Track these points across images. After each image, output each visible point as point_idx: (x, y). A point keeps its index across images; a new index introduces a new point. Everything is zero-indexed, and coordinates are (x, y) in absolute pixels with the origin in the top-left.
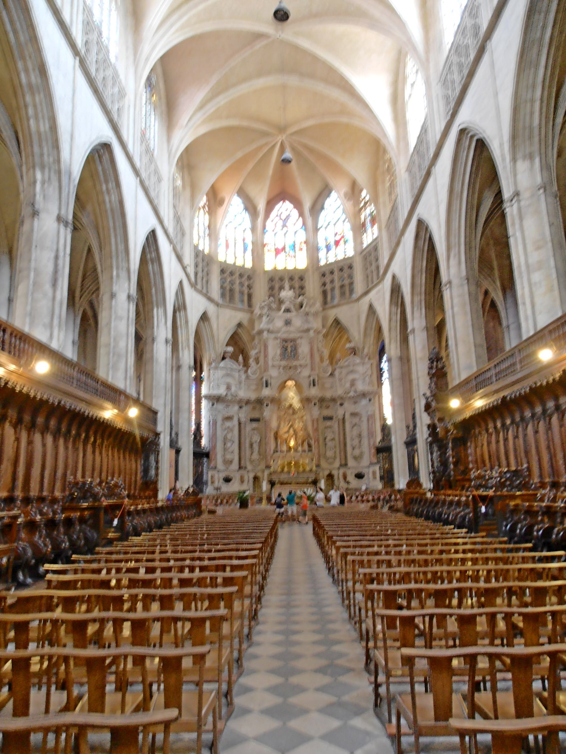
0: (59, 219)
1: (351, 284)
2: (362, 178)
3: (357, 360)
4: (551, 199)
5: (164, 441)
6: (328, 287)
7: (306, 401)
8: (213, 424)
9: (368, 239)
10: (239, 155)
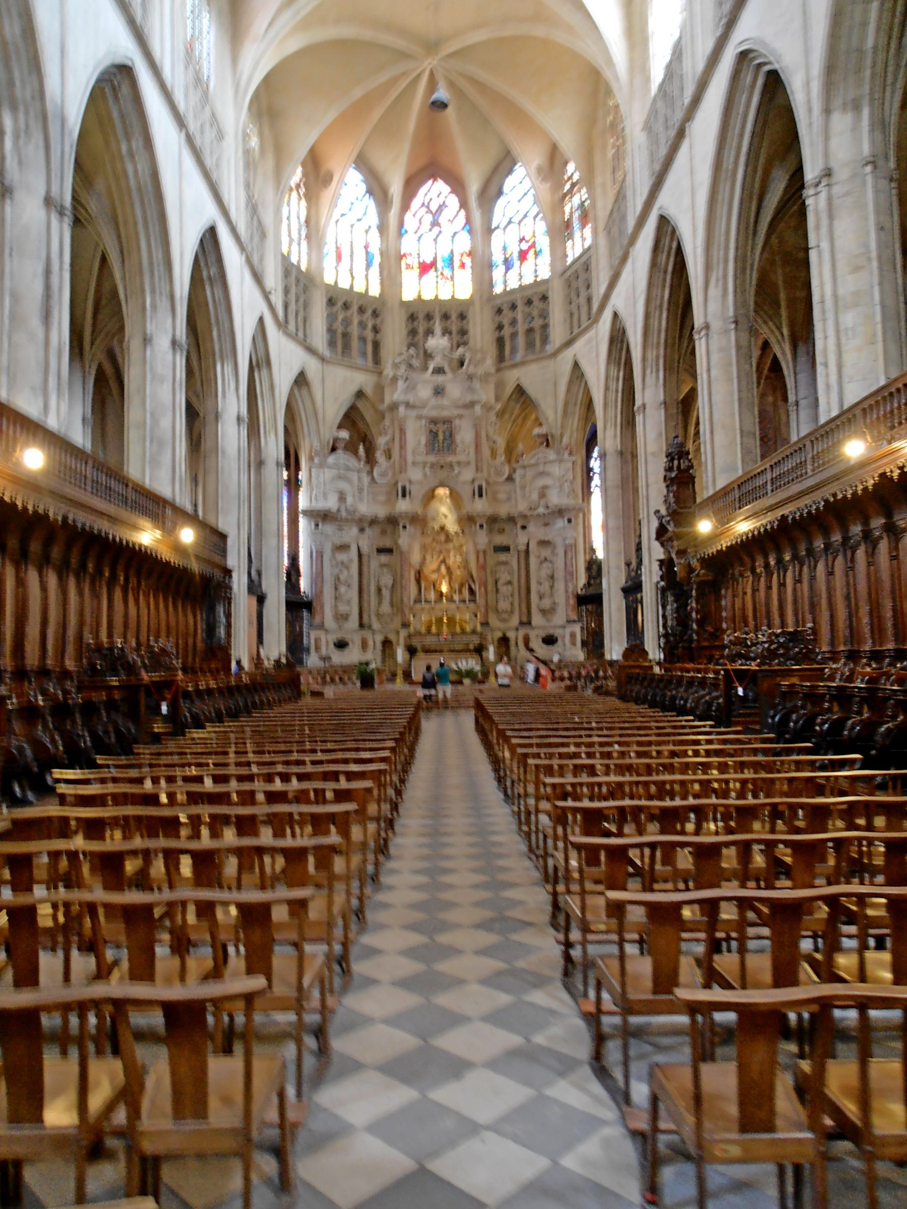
0: (48, 201)
1: (545, 327)
2: (568, 141)
3: (551, 455)
4: (884, 184)
5: (239, 583)
6: (507, 332)
7: (467, 520)
8: (317, 557)
9: (574, 249)
10: (358, 92)
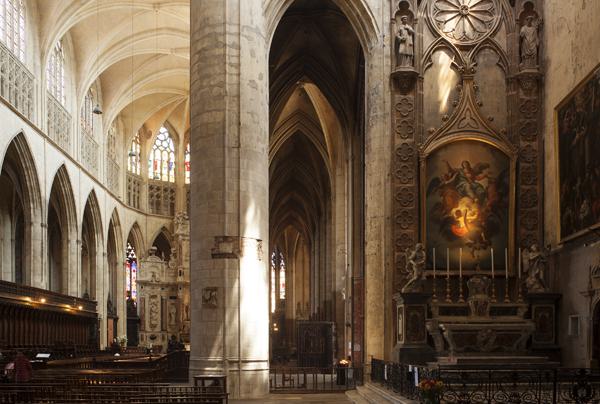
5: (102, 311)
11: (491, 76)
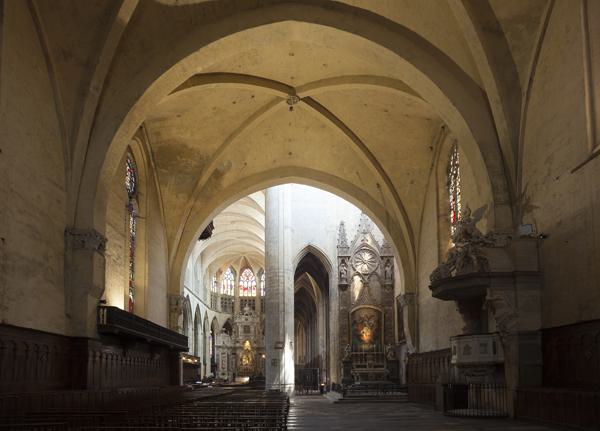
11: (375, 284)
